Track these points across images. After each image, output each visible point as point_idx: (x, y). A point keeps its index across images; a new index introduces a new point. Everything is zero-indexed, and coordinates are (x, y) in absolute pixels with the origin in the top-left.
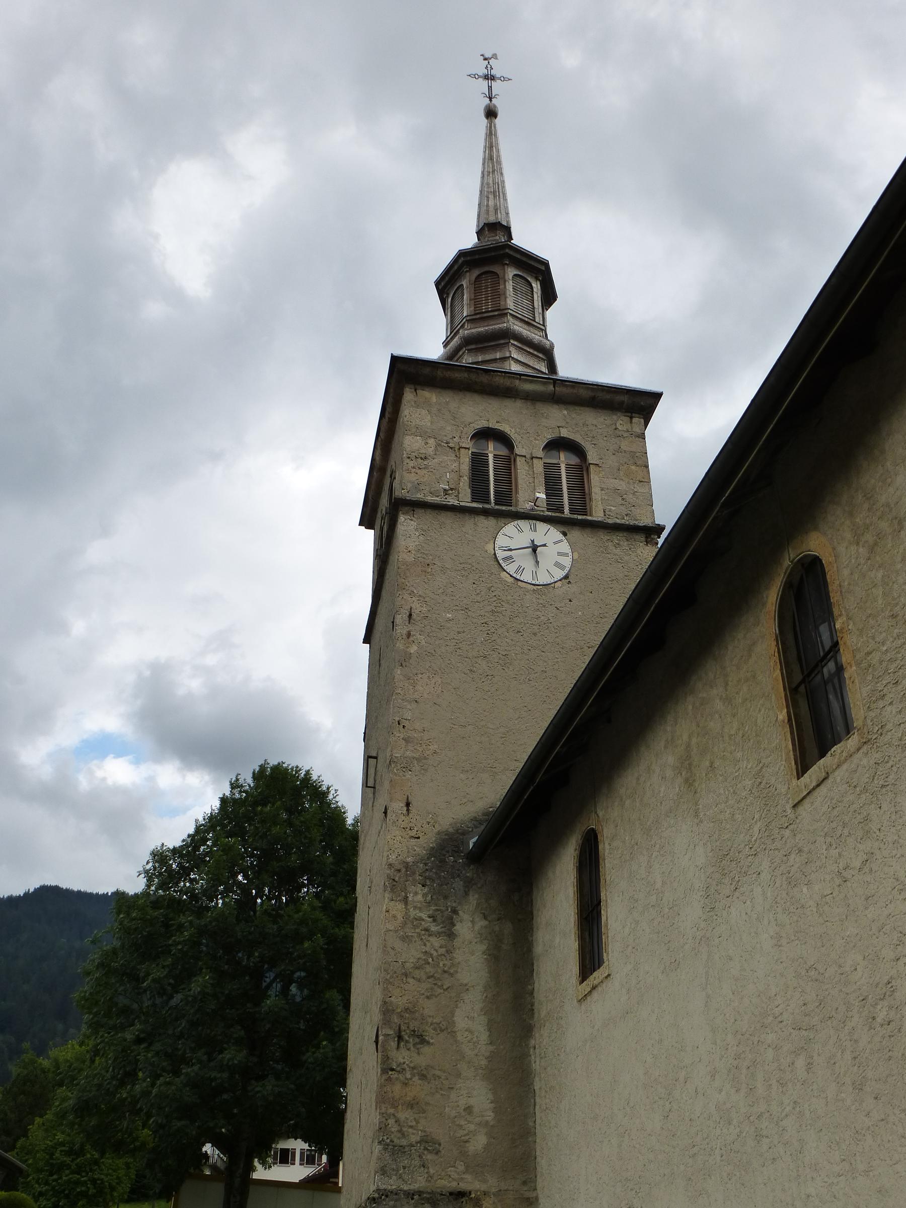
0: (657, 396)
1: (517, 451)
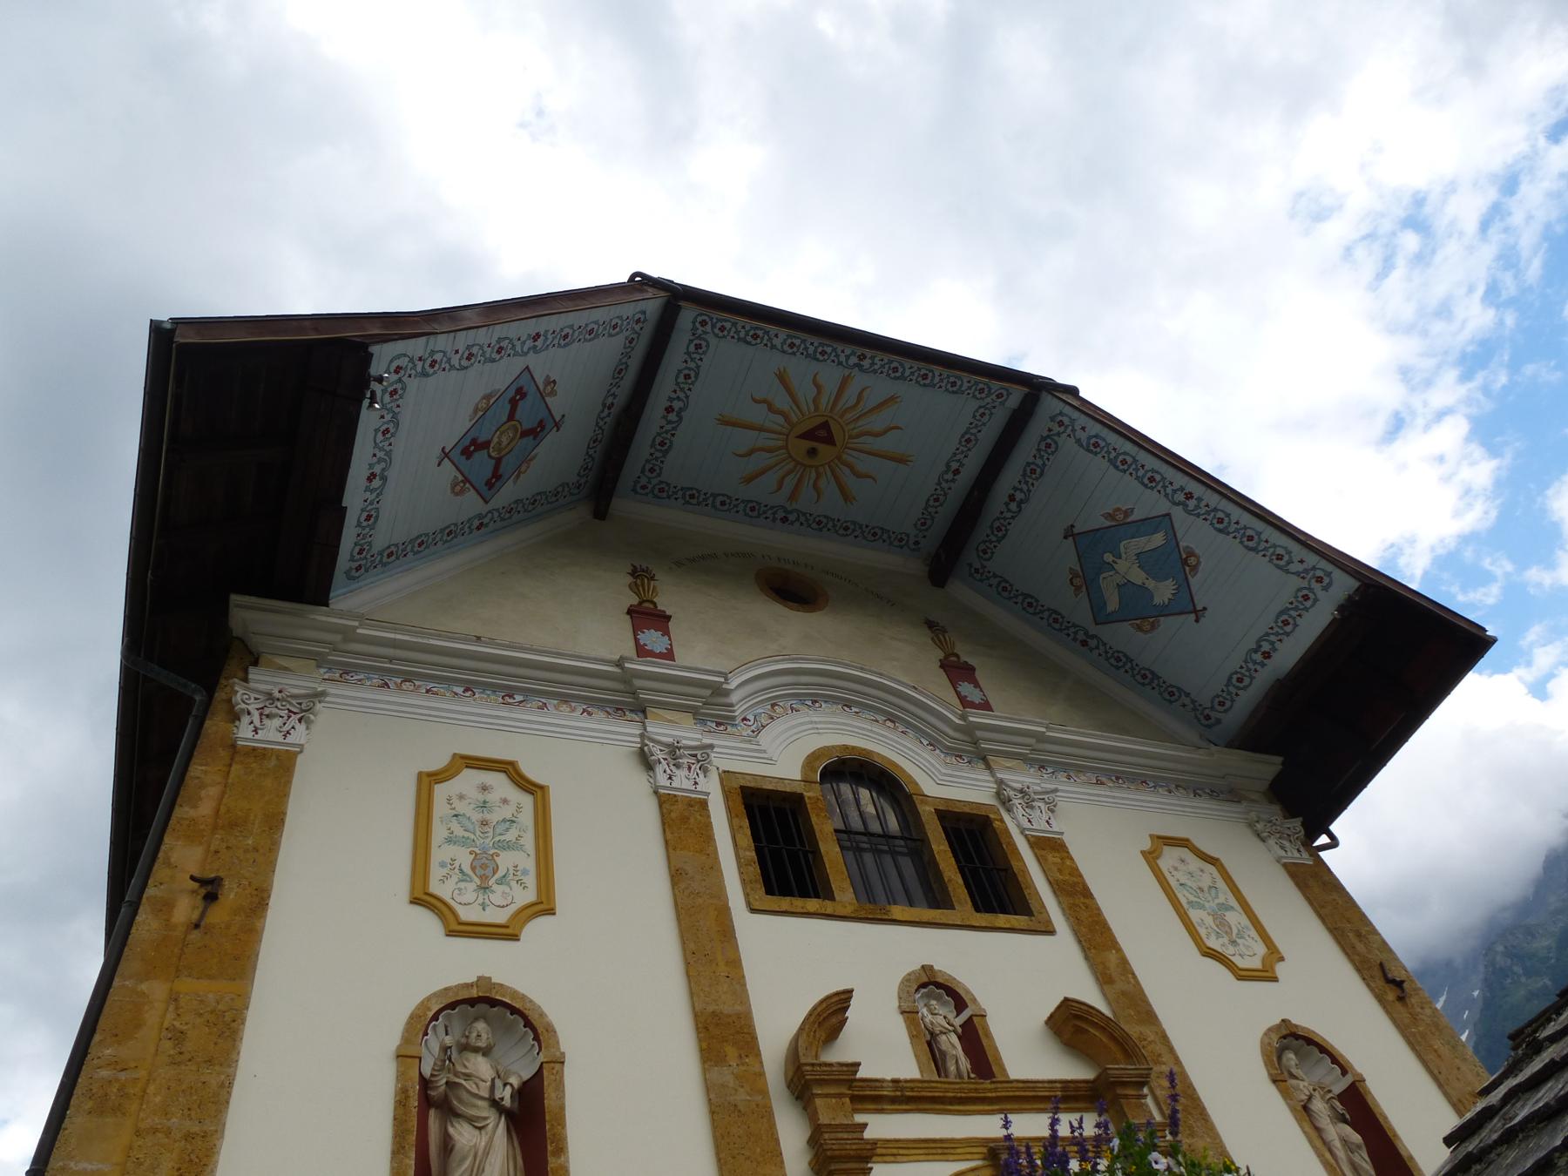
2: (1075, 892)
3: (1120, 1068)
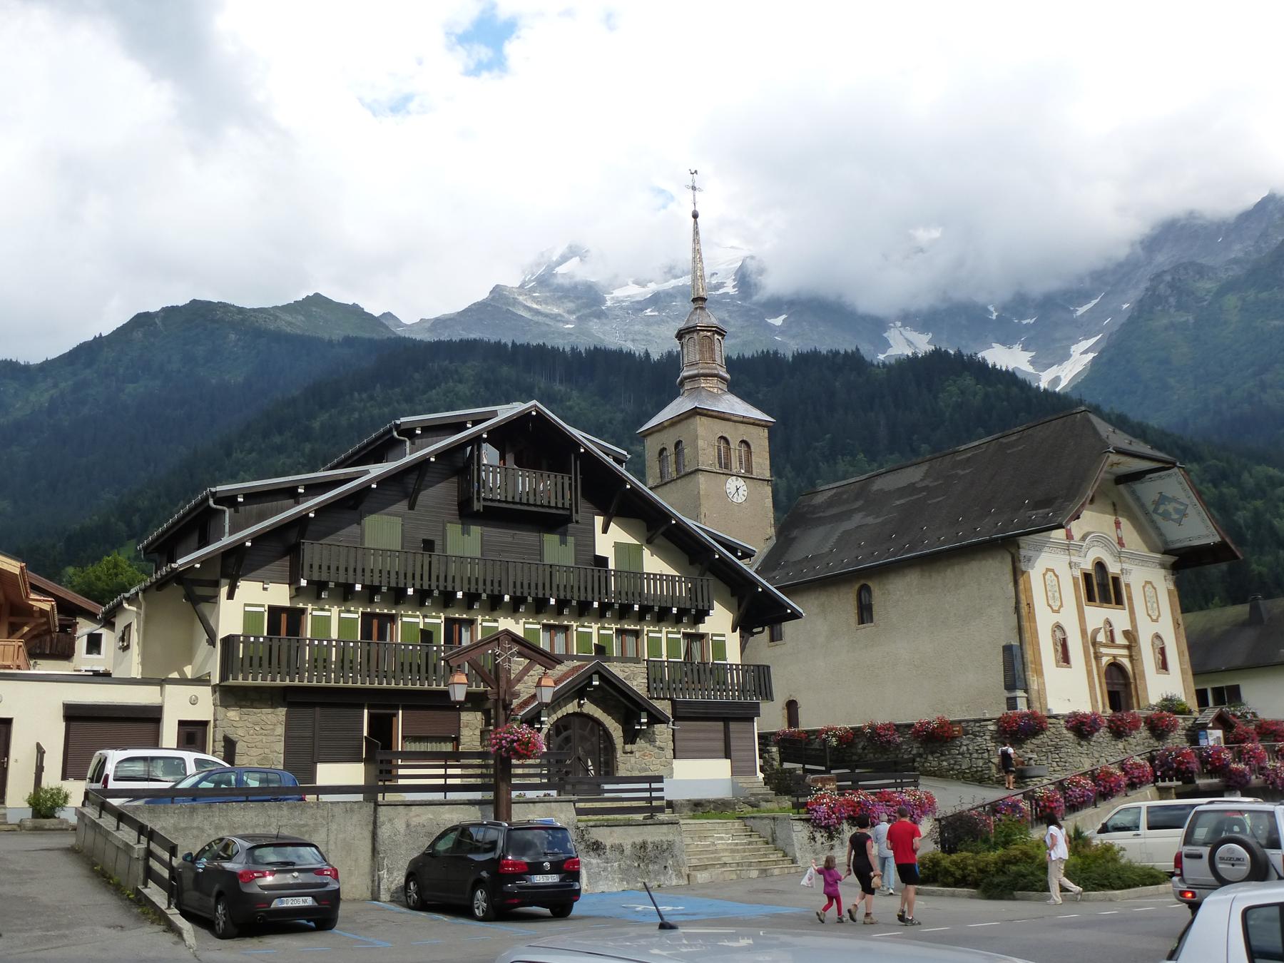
2: (1130, 598)
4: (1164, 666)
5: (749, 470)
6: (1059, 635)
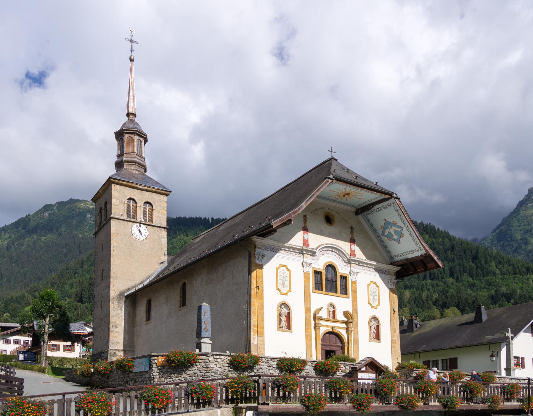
0: (171, 192)
1: (138, 205)
2: (355, 291)
3: (350, 321)
4: (378, 337)
5: (151, 220)
6: (284, 311)
